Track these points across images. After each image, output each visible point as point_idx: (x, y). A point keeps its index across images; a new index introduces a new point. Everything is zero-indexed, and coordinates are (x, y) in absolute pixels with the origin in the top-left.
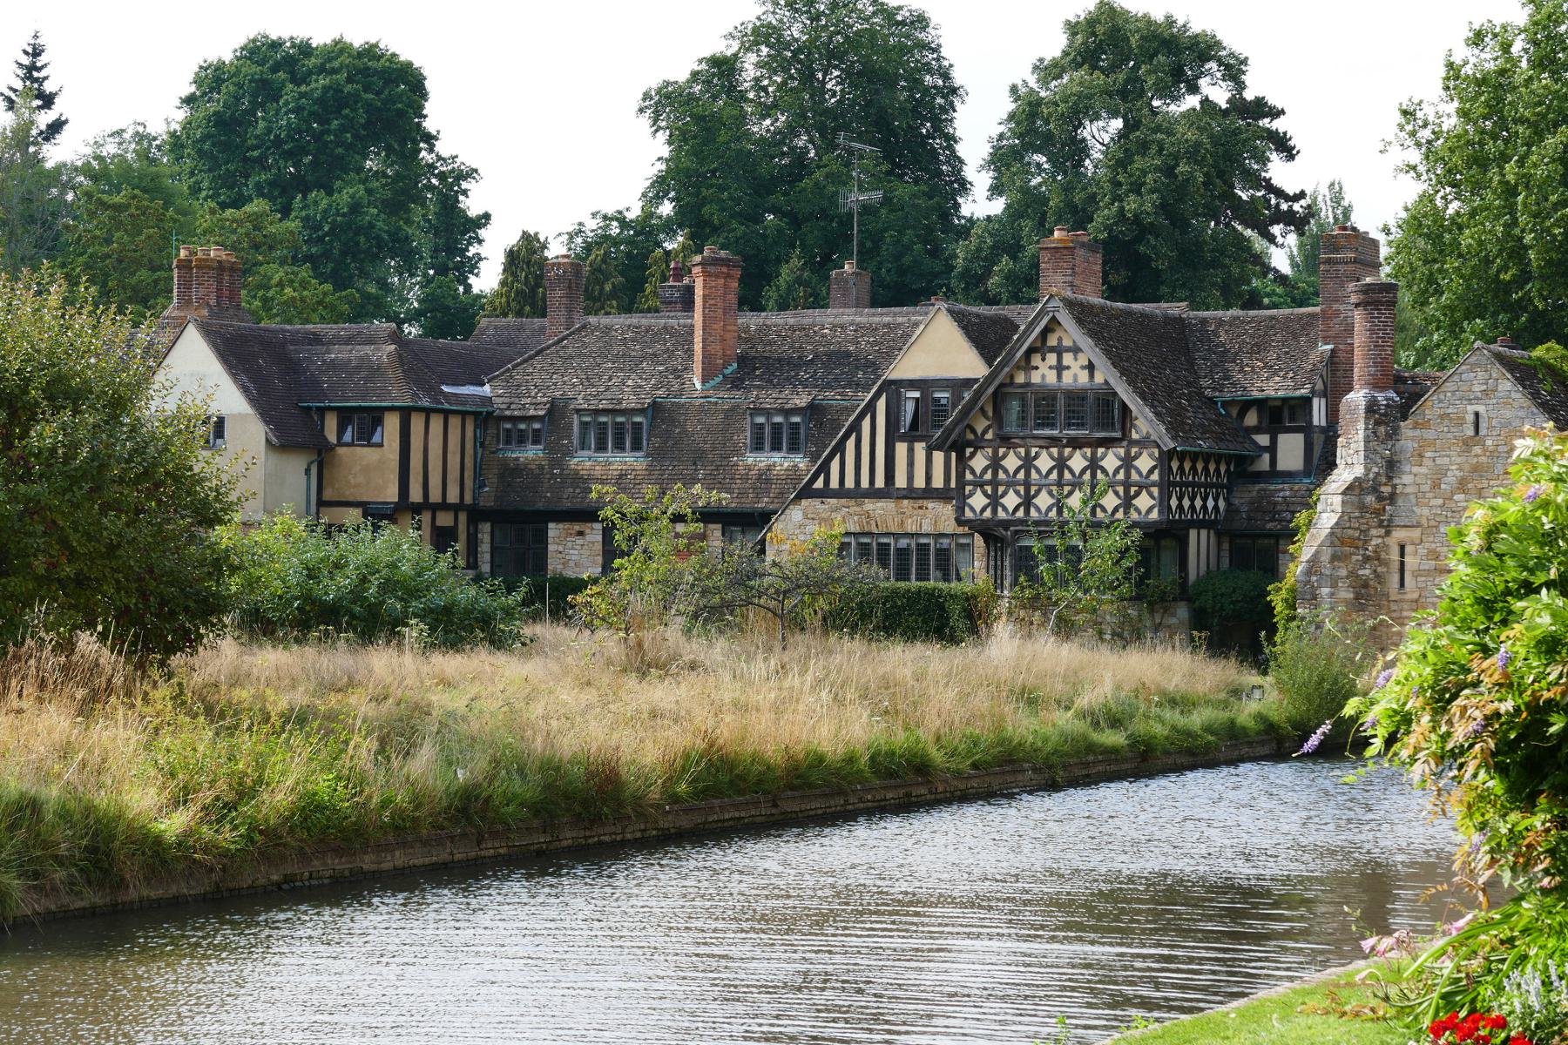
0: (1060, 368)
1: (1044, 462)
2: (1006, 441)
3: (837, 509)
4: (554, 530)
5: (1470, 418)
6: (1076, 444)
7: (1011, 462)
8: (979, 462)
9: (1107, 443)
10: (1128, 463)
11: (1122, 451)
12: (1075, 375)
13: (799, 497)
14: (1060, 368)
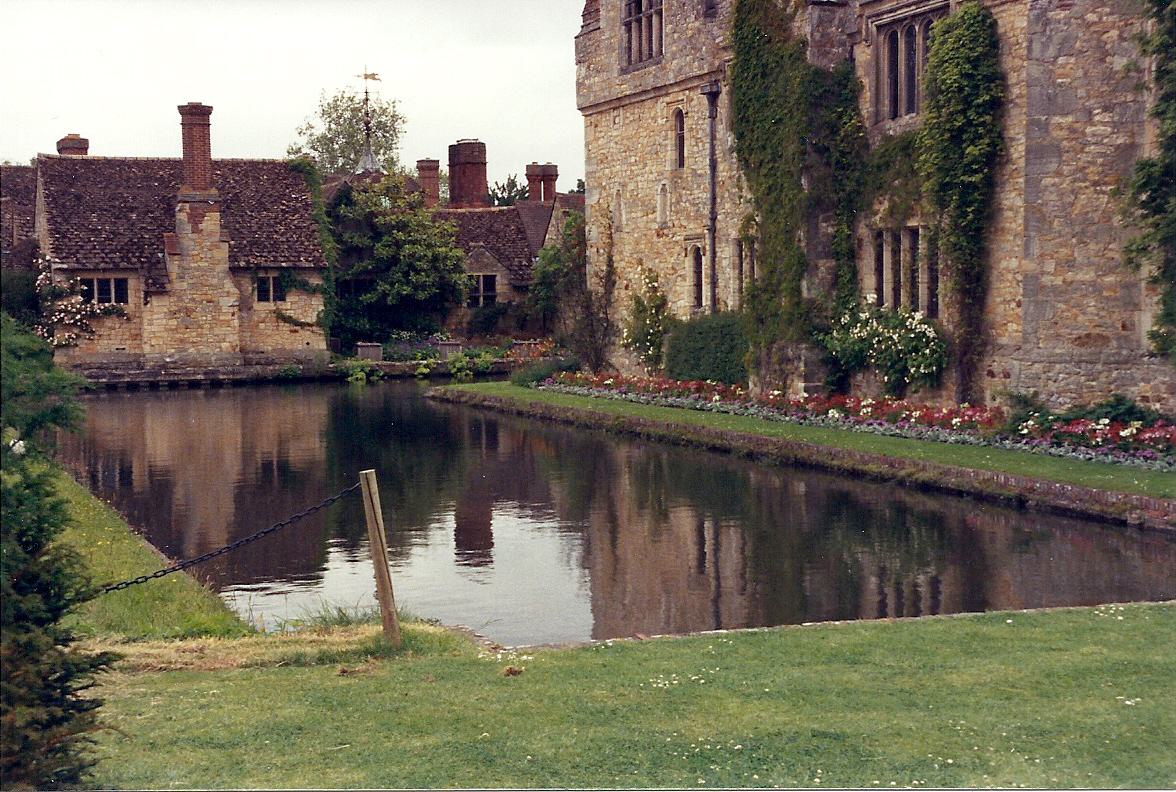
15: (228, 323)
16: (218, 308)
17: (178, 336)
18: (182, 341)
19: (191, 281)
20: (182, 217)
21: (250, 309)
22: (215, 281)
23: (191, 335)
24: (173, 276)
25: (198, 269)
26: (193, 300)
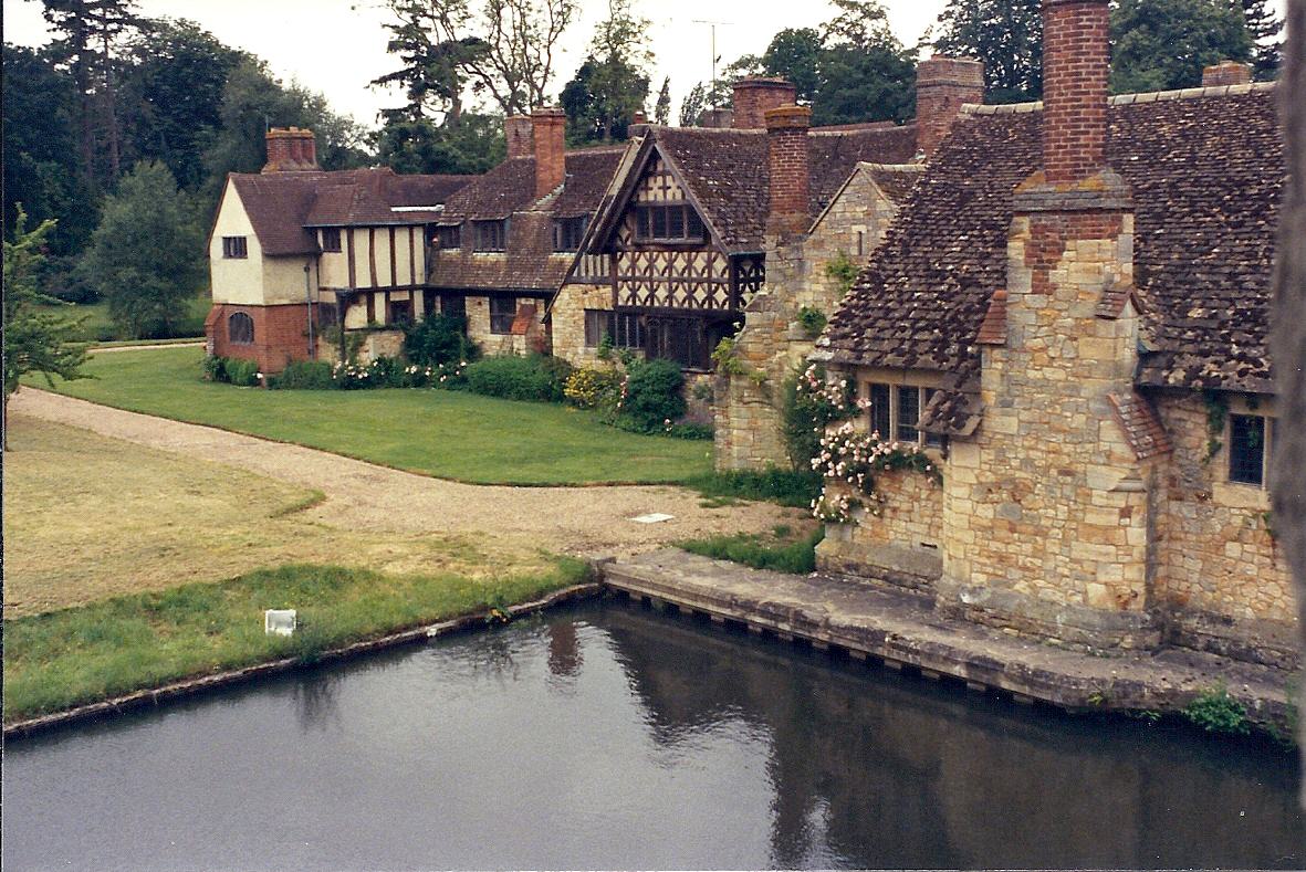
0: (665, 188)
1: (661, 264)
2: (640, 248)
3: (586, 292)
4: (468, 301)
5: (855, 239)
6: (679, 248)
7: (643, 263)
8: (624, 263)
9: (697, 248)
10: (709, 264)
11: (705, 255)
12: (674, 195)
13: (564, 285)
14: (665, 188)
15: (1106, 535)
16: (1083, 493)
17: (994, 546)
18: (1002, 559)
19: (1025, 416)
20: (1016, 250)
21: (1202, 499)
22: (1079, 421)
23: (1021, 550)
24: (991, 398)
25: (1044, 384)
26: (1027, 463)
